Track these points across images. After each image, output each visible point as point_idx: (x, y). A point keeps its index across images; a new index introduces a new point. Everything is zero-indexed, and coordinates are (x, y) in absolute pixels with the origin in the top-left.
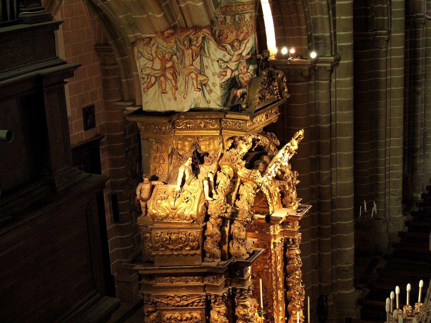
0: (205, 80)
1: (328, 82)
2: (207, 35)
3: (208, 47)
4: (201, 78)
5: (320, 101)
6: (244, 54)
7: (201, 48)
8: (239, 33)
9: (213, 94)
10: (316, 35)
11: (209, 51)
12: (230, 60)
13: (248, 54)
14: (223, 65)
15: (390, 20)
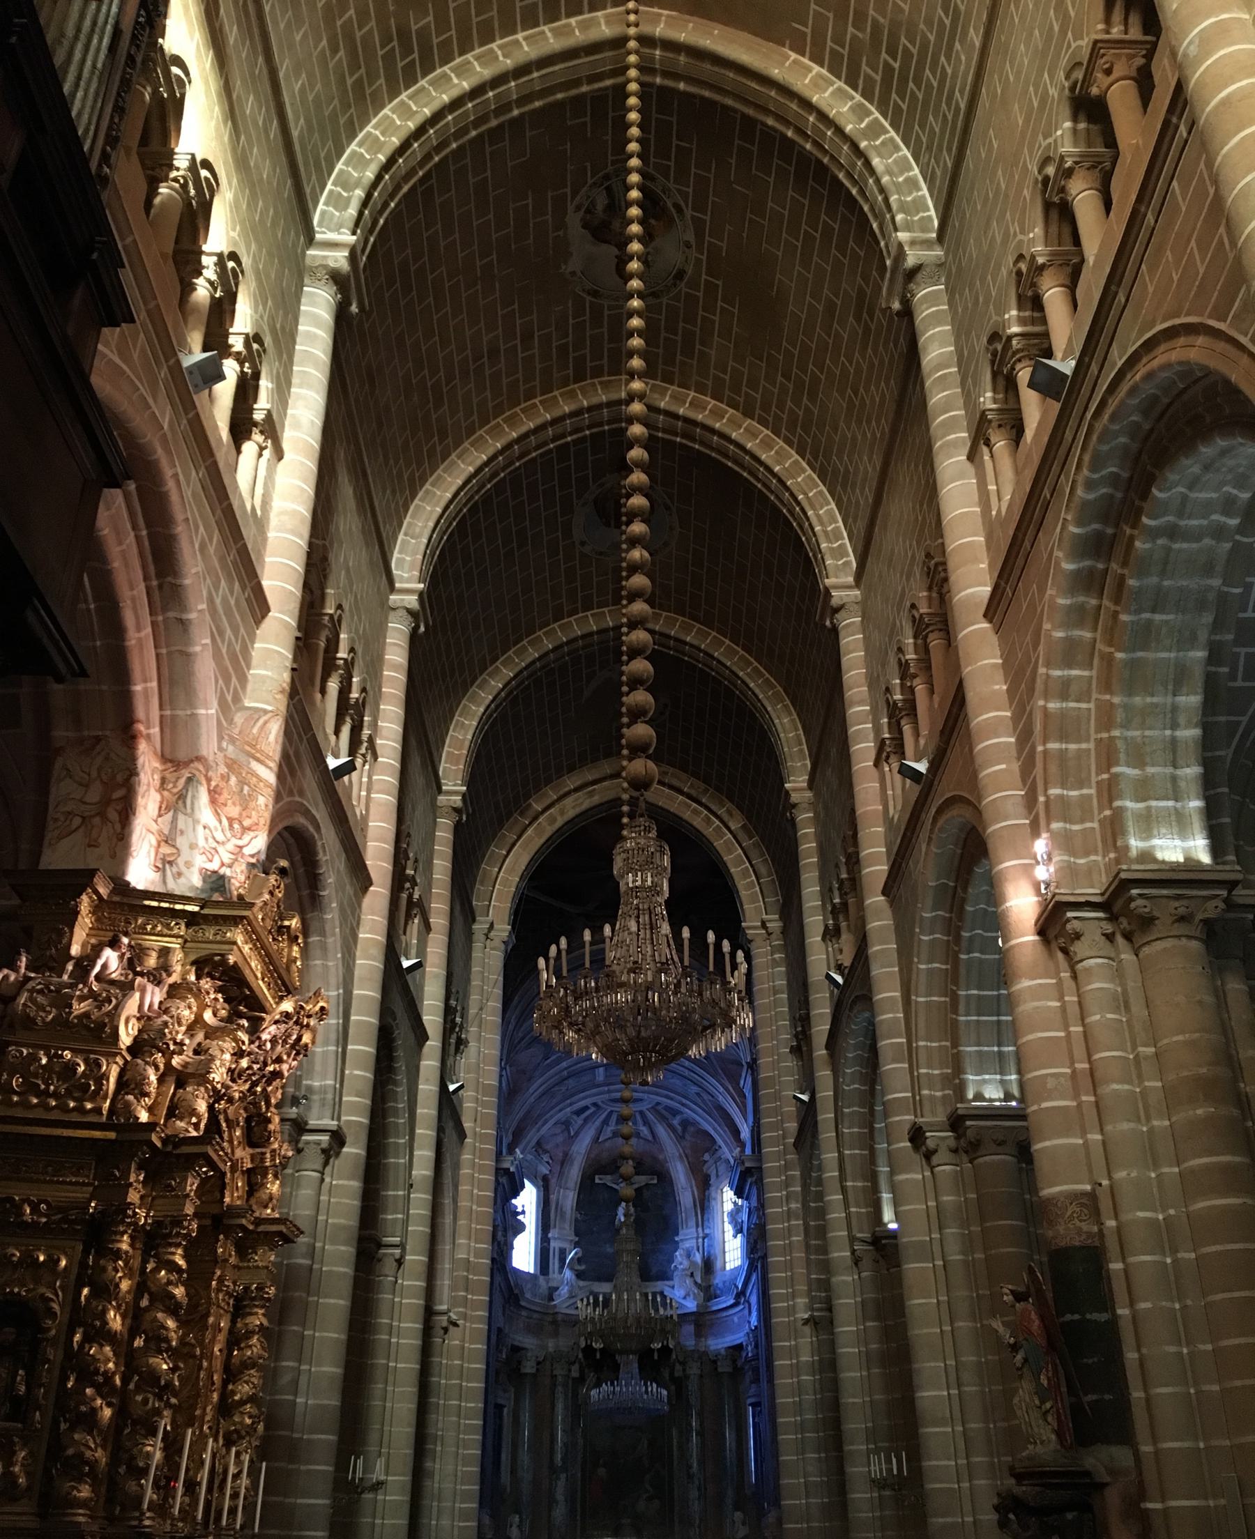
0: (173, 854)
1: (317, 1175)
2: (197, 773)
3: (193, 797)
4: (166, 850)
5: (298, 1212)
6: (247, 851)
7: (179, 798)
8: (244, 814)
9: (182, 880)
10: (309, 1082)
11: (193, 804)
12: (223, 843)
13: (252, 856)
14: (211, 840)
15: (406, 1222)
